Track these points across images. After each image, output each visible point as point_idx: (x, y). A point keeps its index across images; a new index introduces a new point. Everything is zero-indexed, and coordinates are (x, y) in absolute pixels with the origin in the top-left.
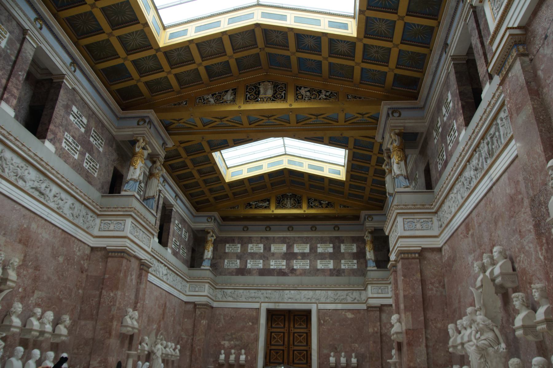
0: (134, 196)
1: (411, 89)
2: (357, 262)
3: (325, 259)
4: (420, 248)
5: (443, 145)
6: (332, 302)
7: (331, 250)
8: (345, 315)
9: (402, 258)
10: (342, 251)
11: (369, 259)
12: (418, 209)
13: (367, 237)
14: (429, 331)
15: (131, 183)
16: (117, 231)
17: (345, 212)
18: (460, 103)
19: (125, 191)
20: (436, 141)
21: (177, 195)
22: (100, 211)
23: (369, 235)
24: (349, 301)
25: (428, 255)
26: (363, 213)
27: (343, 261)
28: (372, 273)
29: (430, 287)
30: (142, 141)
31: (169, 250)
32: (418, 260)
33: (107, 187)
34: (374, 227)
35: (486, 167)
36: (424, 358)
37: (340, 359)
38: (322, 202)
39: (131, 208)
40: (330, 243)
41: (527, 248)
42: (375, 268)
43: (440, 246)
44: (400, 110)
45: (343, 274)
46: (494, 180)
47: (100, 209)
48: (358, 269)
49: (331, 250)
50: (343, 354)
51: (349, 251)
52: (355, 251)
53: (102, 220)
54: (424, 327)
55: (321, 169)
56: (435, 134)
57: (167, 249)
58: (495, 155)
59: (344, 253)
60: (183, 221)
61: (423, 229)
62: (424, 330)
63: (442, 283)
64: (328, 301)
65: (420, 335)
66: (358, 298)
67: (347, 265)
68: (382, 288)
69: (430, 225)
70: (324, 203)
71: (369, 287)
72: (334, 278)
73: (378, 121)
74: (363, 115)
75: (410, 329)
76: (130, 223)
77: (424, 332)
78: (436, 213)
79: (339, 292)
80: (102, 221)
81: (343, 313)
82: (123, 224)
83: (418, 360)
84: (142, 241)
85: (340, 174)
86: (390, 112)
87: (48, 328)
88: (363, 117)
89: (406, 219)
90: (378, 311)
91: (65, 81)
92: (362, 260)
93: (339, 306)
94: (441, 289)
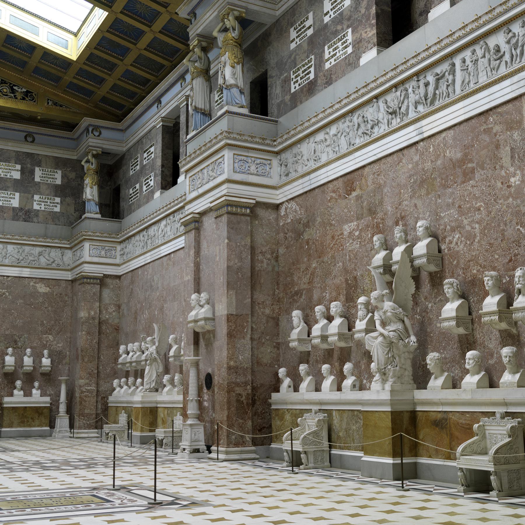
3: (6, 190)
4: (254, 202)
5: (313, 57)
7: (17, 175)
8: (35, 287)
9: (228, 213)
10: (37, 179)
11: (89, 200)
12: (256, 143)
13: (88, 161)
17: (55, 113)
18: (374, 8)
20: (293, 46)
23: (93, 160)
25: (261, 212)
26: (86, 121)
27: (36, 197)
28: (93, 222)
29: (260, 257)
34: (102, 148)
35: (412, 115)
36: (248, 354)
37: (23, 360)
38: (15, 88)
40: (16, 163)
41: (468, 228)
42: (99, 216)
43: (278, 202)
45: (35, 220)
46: (426, 135)
48: (61, 213)
49: (17, 175)
50: (28, 351)
52: (59, 182)
55: (35, 31)
56: (293, 34)
58: (438, 104)
59: (39, 183)
61: (258, 174)
62: (250, 316)
63: (275, 254)
64: (7, 262)
65: (246, 324)
66: (58, 261)
67: (43, 204)
68: (107, 248)
70: (20, 90)
71: (87, 245)
72: (20, 225)
75: (232, 315)
78: (278, 153)
79: (27, 248)
81: (32, 284)
83: (240, 357)
85: (67, 48)
89: (238, 155)
90: (98, 284)
92: (68, 200)
93: (26, 273)
94: (273, 261)
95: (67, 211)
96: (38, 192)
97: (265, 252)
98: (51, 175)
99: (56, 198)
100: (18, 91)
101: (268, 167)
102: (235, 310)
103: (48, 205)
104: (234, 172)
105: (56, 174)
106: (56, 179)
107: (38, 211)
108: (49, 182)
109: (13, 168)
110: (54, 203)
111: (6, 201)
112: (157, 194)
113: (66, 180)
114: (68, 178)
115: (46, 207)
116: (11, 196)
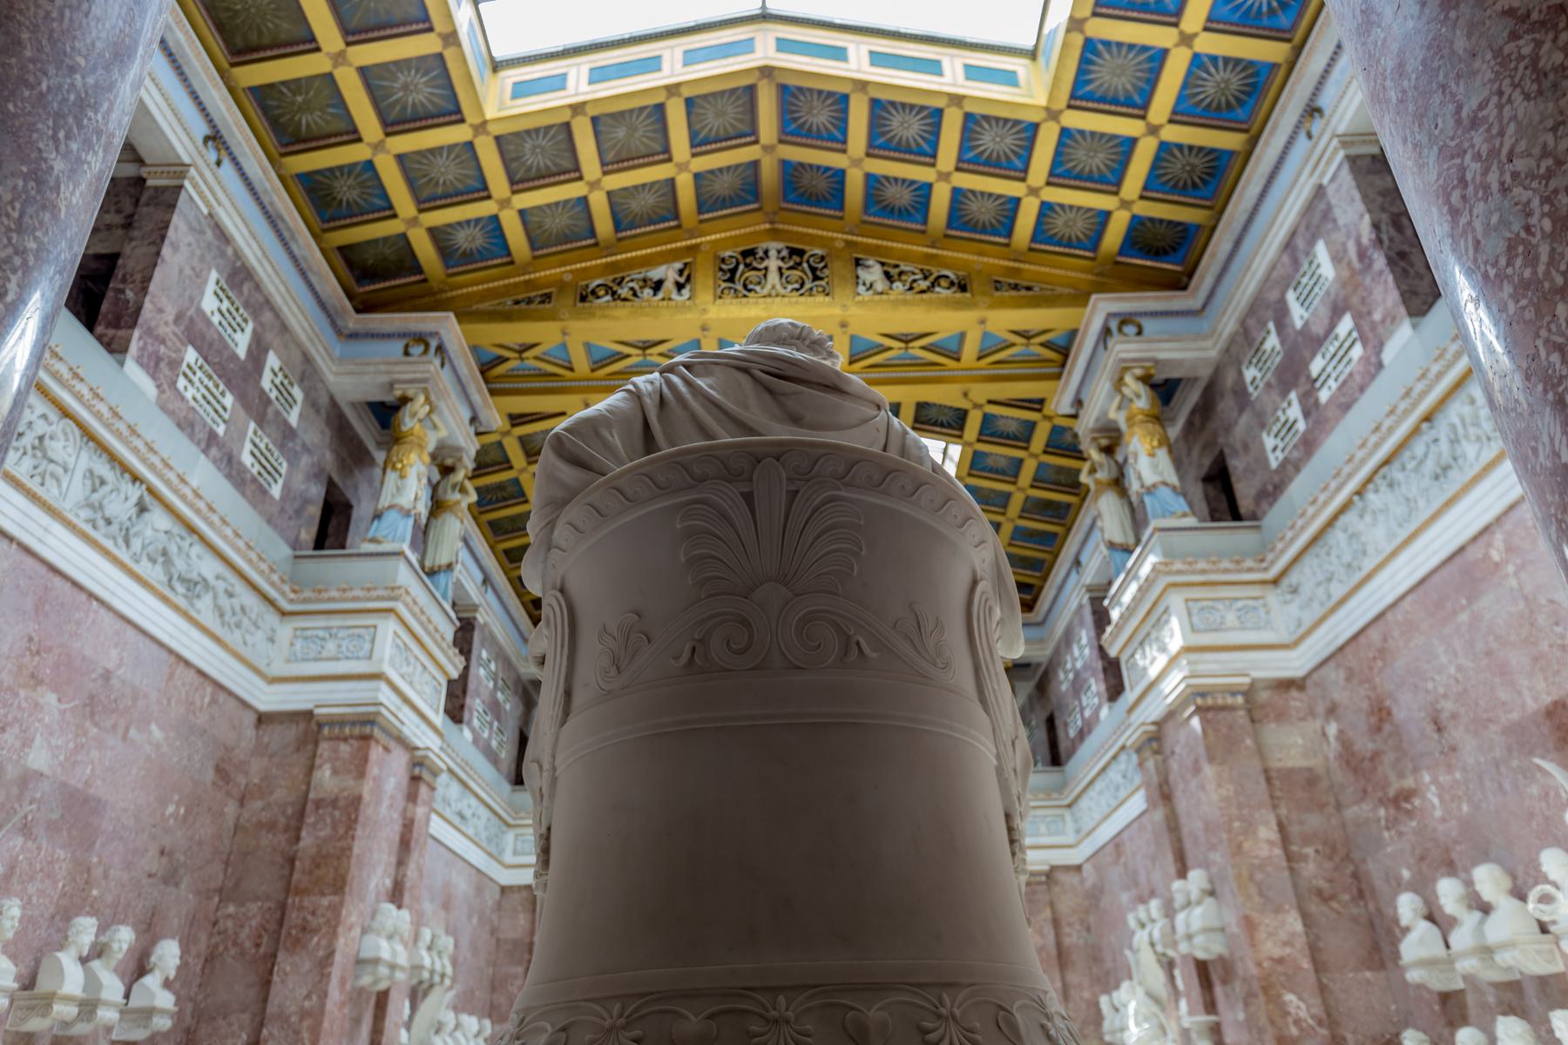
0: (400, 554)
4: (1247, 680)
15: (391, 516)
16: (347, 658)
19: (374, 540)
21: (487, 581)
22: (291, 601)
30: (422, 399)
31: (467, 734)
33: (308, 535)
39: (393, 589)
47: (292, 596)
53: (296, 629)
57: (461, 730)
60: (501, 656)
73: (1066, 356)
74: (1028, 337)
76: (390, 635)
78: (1275, 582)
80: (298, 633)
82: (367, 638)
84: (419, 693)
86: (1114, 325)
87: (112, 988)
88: (1027, 345)
89: (1196, 600)
91: (187, 184)
101: (1262, 611)
112: (1104, 712)
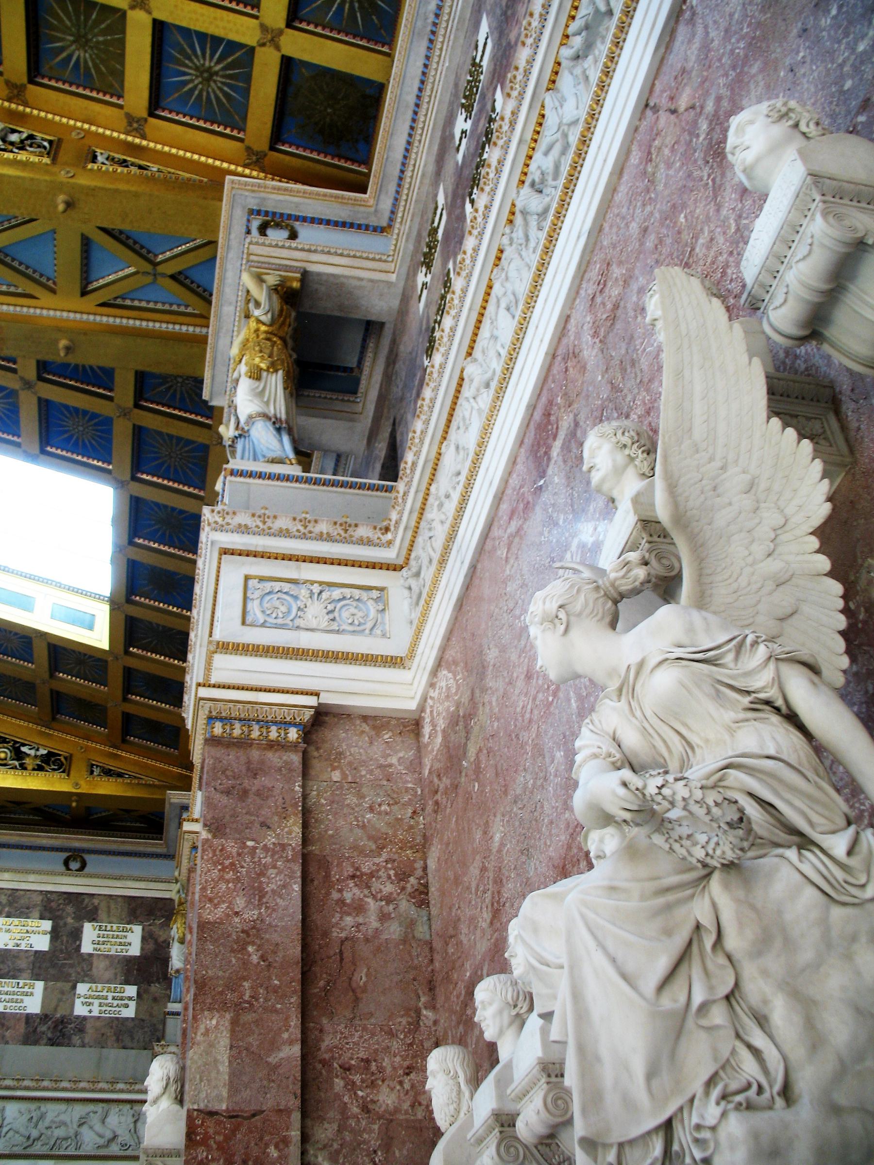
1: (347, 159)
2: (139, 994)
3: (14, 977)
4: (312, 701)
6: (17, 1150)
7: (42, 943)
10: (87, 947)
14: (325, 1132)
24: (88, 1148)
27: (82, 988)
32: (295, 758)
38: (24, 749)
40: (42, 918)
44: (297, 225)
45: (76, 1039)
49: (42, 943)
51: (114, 950)
52: (135, 950)
54: (294, 1103)
55: (26, 603)
59: (91, 955)
62: (296, 1117)
63: (412, 880)
65: (273, 1153)
66: (124, 1136)
67: (96, 1002)
69: (372, 613)
70: (32, 752)
72: (41, 1052)
75: (211, 1114)
77: (295, 1134)
79: (52, 1111)
85: (91, 628)
86: (255, 224)
89: (262, 579)
94: (405, 905)
95: (151, 1015)
96: (87, 976)
97: (372, 875)
98: (118, 936)
99: (127, 987)
100: (28, 755)
102: (225, 1093)
103: (107, 1005)
104: (244, 623)
105: (129, 934)
106: (130, 944)
107: (85, 1018)
108: (113, 953)
109: (35, 929)
110: (122, 999)
111: (12, 1001)
113: (151, 946)
114: (156, 941)
115: (104, 1009)
116: (26, 989)
